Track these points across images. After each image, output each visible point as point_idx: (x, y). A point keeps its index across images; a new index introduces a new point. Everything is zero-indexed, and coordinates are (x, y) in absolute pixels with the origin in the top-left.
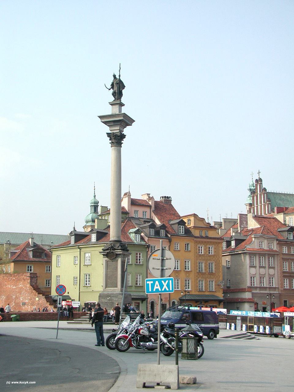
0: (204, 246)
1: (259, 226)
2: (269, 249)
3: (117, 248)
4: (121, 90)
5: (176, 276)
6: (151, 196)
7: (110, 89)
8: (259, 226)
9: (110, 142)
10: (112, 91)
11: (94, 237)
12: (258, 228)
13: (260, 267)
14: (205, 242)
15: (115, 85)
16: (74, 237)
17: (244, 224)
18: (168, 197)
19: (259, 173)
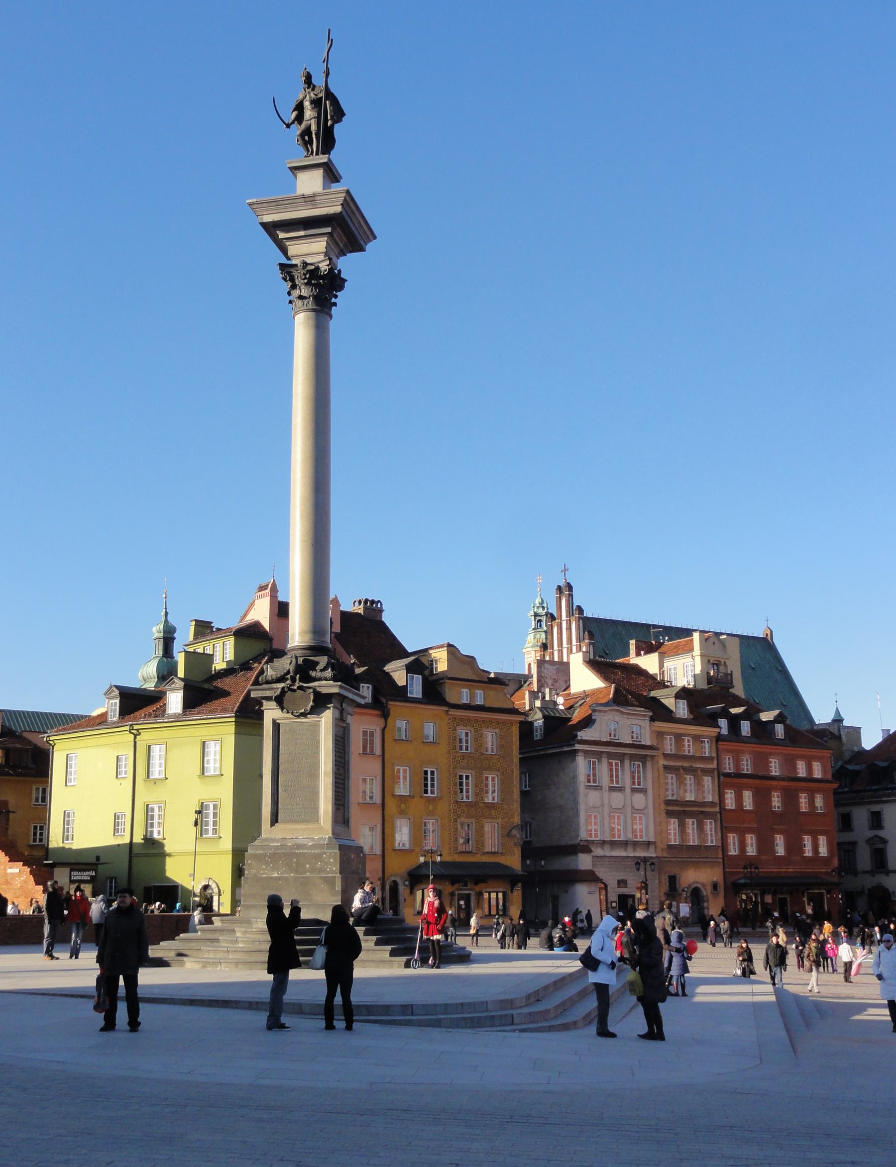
0: (473, 731)
2: (631, 742)
4: (330, 123)
5: (402, 811)
7: (288, 126)
11: (175, 701)
13: (612, 789)
14: (476, 721)
15: (307, 104)
16: (118, 701)
18: (373, 602)
19: (565, 570)
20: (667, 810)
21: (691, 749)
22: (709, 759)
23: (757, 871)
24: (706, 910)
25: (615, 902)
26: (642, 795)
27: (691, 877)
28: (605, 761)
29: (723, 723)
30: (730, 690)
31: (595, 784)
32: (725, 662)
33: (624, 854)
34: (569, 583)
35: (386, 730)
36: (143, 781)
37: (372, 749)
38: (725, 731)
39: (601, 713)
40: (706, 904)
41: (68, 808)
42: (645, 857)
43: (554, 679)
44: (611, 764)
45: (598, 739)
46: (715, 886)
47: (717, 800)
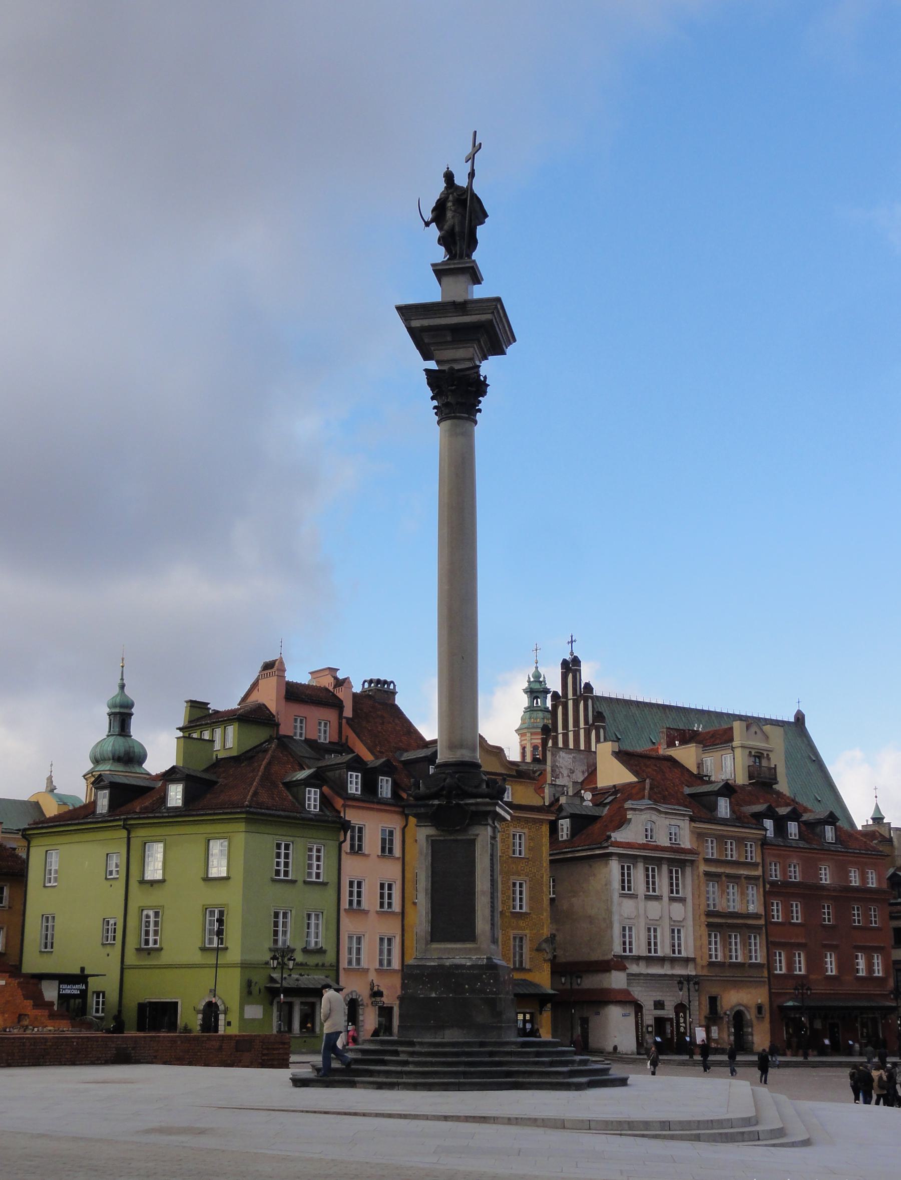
1: (634, 779)
2: (670, 845)
3: (475, 791)
6: (341, 675)
7: (427, 224)
8: (634, 779)
9: (435, 403)
12: (630, 785)
13: (648, 898)
17: (563, 777)
18: (385, 682)
19: (572, 642)
20: (708, 922)
21: (734, 853)
22: (755, 865)
23: (809, 992)
24: (750, 1037)
25: (651, 1026)
26: (681, 904)
28: (641, 867)
29: (769, 824)
30: (774, 786)
31: (629, 892)
32: (768, 755)
34: (576, 657)
35: (406, 830)
36: (137, 883)
37: (391, 850)
38: (770, 834)
39: (637, 812)
41: (48, 911)
42: (688, 975)
43: (571, 769)
44: (647, 870)
45: (634, 841)
46: (760, 1008)
47: (761, 911)
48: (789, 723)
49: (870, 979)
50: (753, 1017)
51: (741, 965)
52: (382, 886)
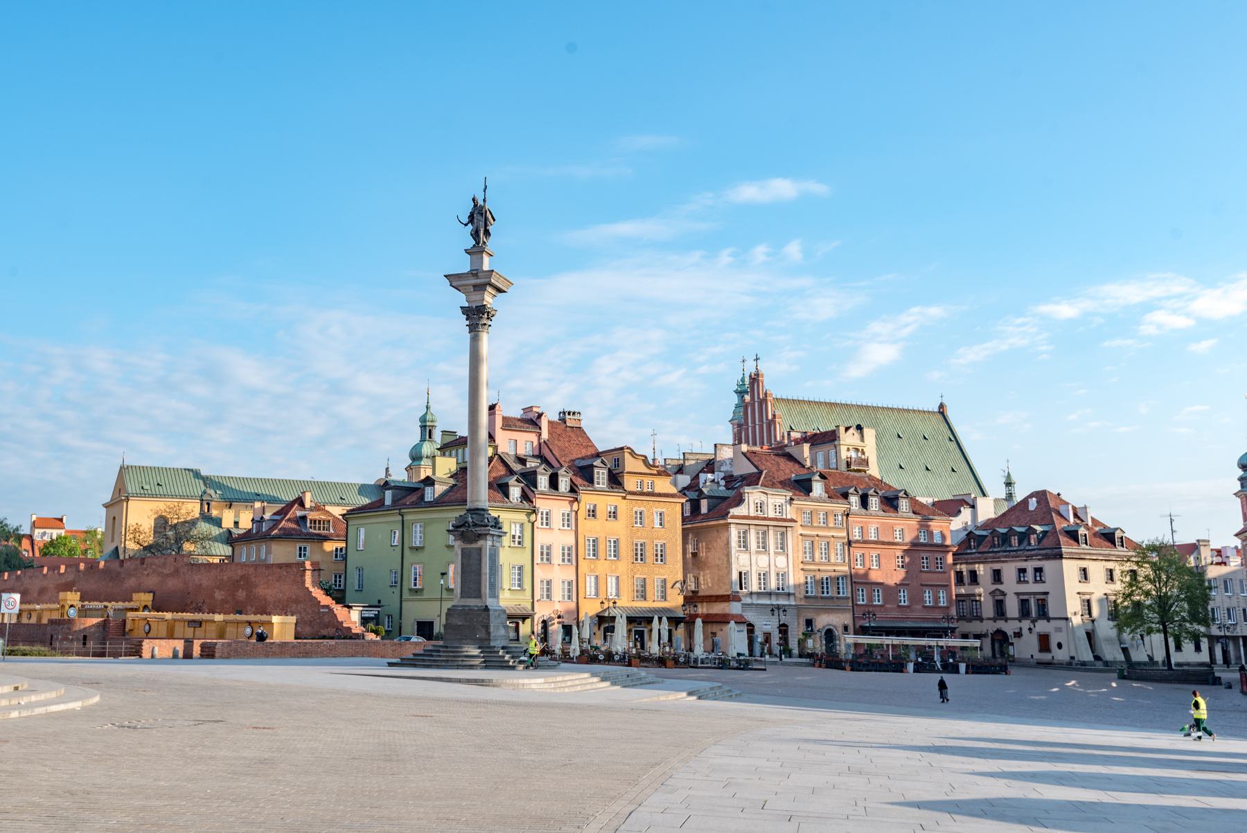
3: (480, 523)
10: (470, 227)
12: (750, 475)
18: (574, 413)
19: (757, 359)
24: (838, 647)
27: (823, 621)
29: (854, 499)
33: (768, 602)
40: (838, 642)
46: (846, 628)
48: (933, 413)
49: (936, 607)
50: (840, 632)
51: (832, 598)
52: (563, 549)
